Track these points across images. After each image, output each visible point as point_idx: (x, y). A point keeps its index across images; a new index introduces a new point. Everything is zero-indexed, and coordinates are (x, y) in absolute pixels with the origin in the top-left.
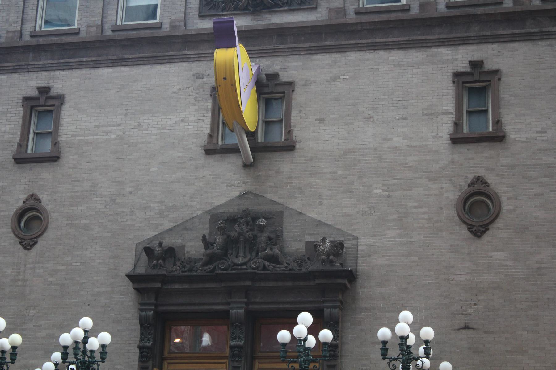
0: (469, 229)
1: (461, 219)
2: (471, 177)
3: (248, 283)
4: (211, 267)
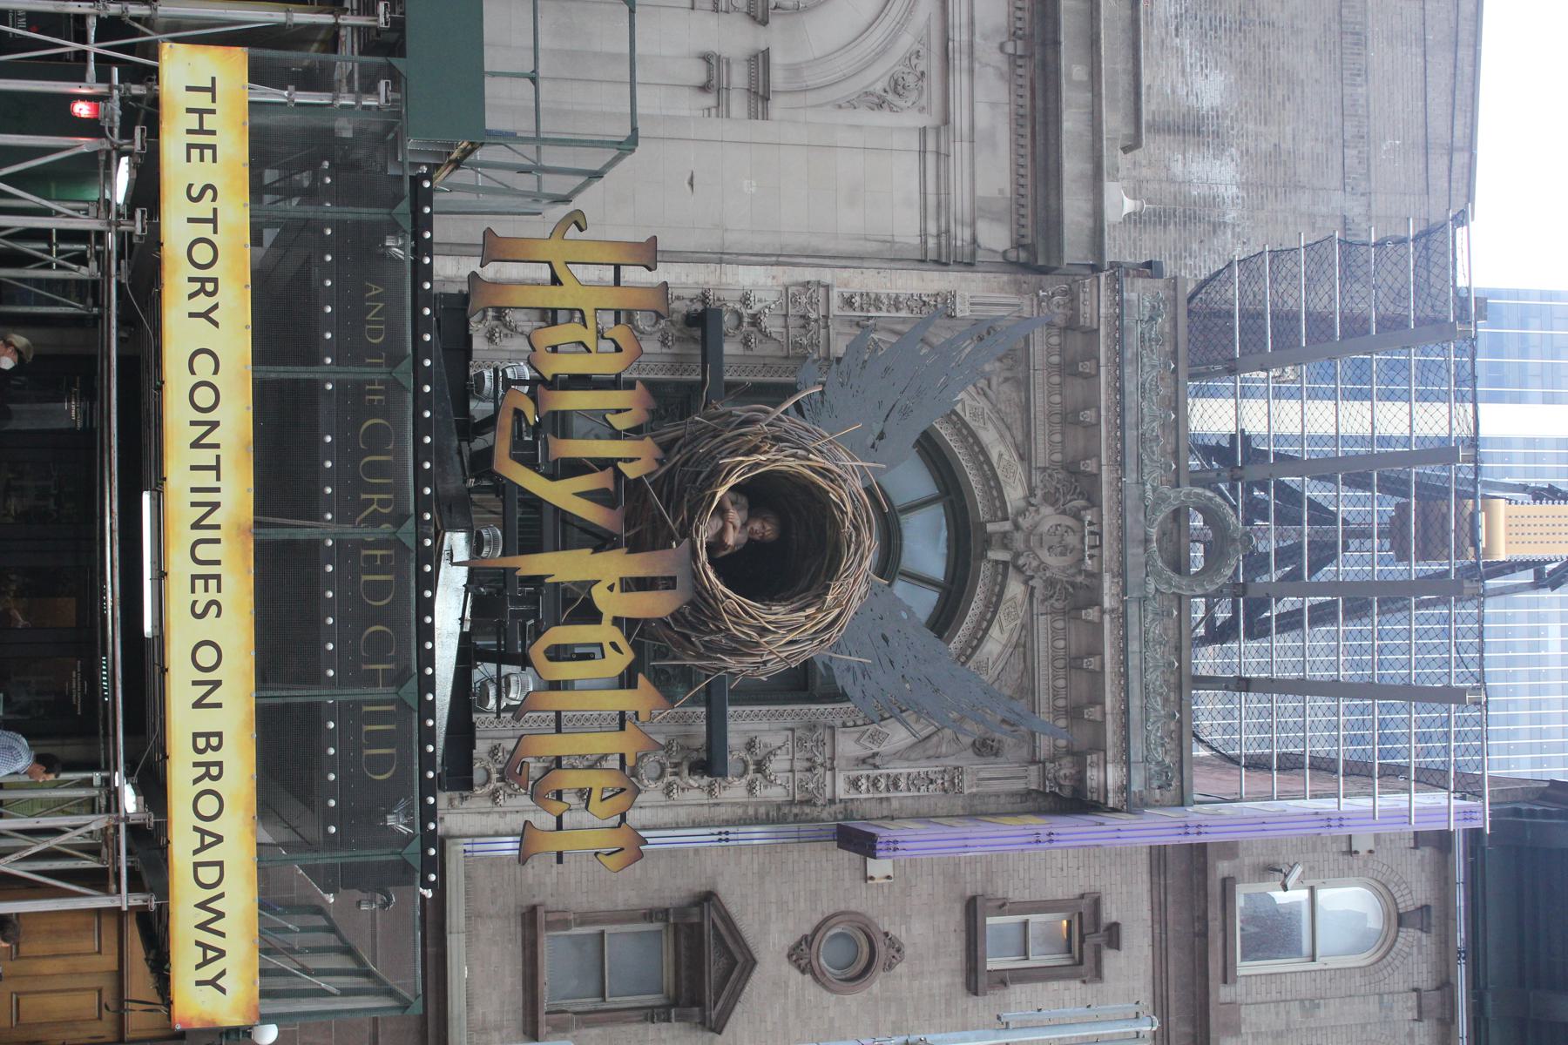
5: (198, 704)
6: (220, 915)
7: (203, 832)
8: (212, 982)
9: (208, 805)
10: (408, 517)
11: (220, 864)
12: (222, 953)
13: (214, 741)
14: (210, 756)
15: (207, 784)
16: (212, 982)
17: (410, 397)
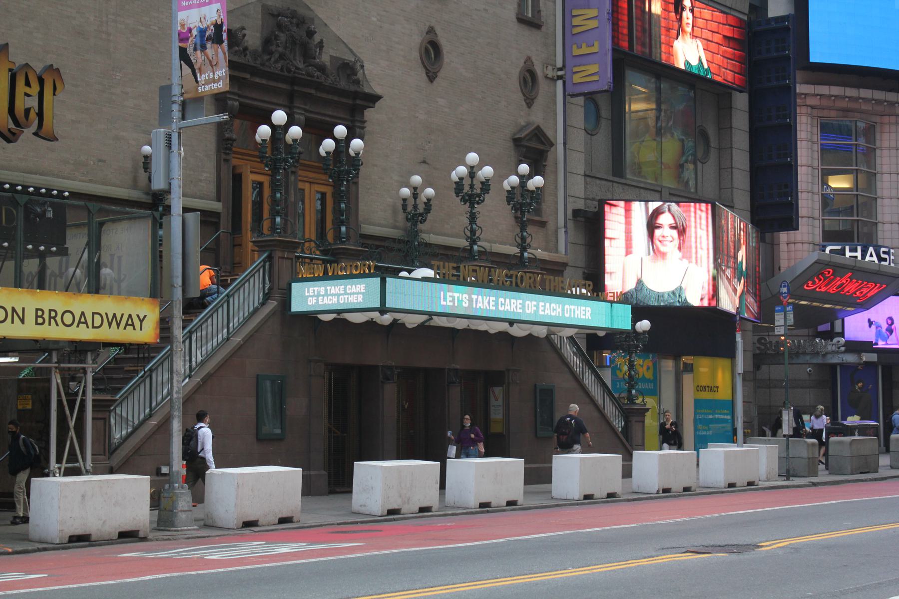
0: (427, 73)
1: (423, 63)
2: (428, 24)
3: (313, 91)
4: (279, 65)
5: (22, 321)
6: (114, 316)
7: (80, 322)
8: (141, 321)
9: (68, 319)
10: (13, 197)
11: (94, 314)
12: (130, 316)
13: (40, 313)
14: (46, 316)
15: (58, 319)
16: (141, 321)
17: (32, 197)
